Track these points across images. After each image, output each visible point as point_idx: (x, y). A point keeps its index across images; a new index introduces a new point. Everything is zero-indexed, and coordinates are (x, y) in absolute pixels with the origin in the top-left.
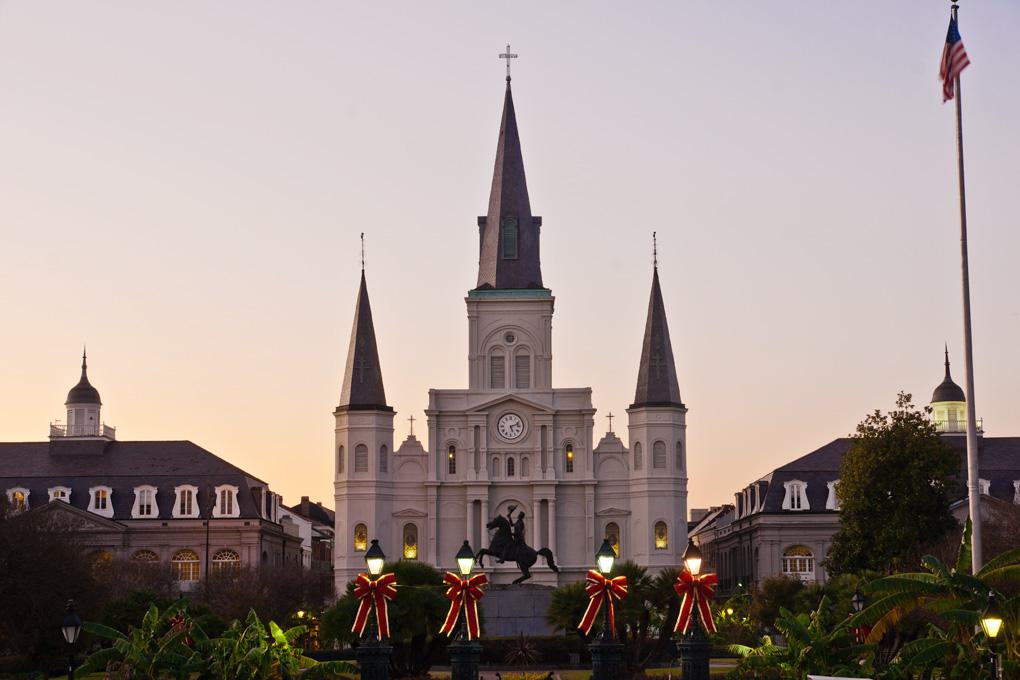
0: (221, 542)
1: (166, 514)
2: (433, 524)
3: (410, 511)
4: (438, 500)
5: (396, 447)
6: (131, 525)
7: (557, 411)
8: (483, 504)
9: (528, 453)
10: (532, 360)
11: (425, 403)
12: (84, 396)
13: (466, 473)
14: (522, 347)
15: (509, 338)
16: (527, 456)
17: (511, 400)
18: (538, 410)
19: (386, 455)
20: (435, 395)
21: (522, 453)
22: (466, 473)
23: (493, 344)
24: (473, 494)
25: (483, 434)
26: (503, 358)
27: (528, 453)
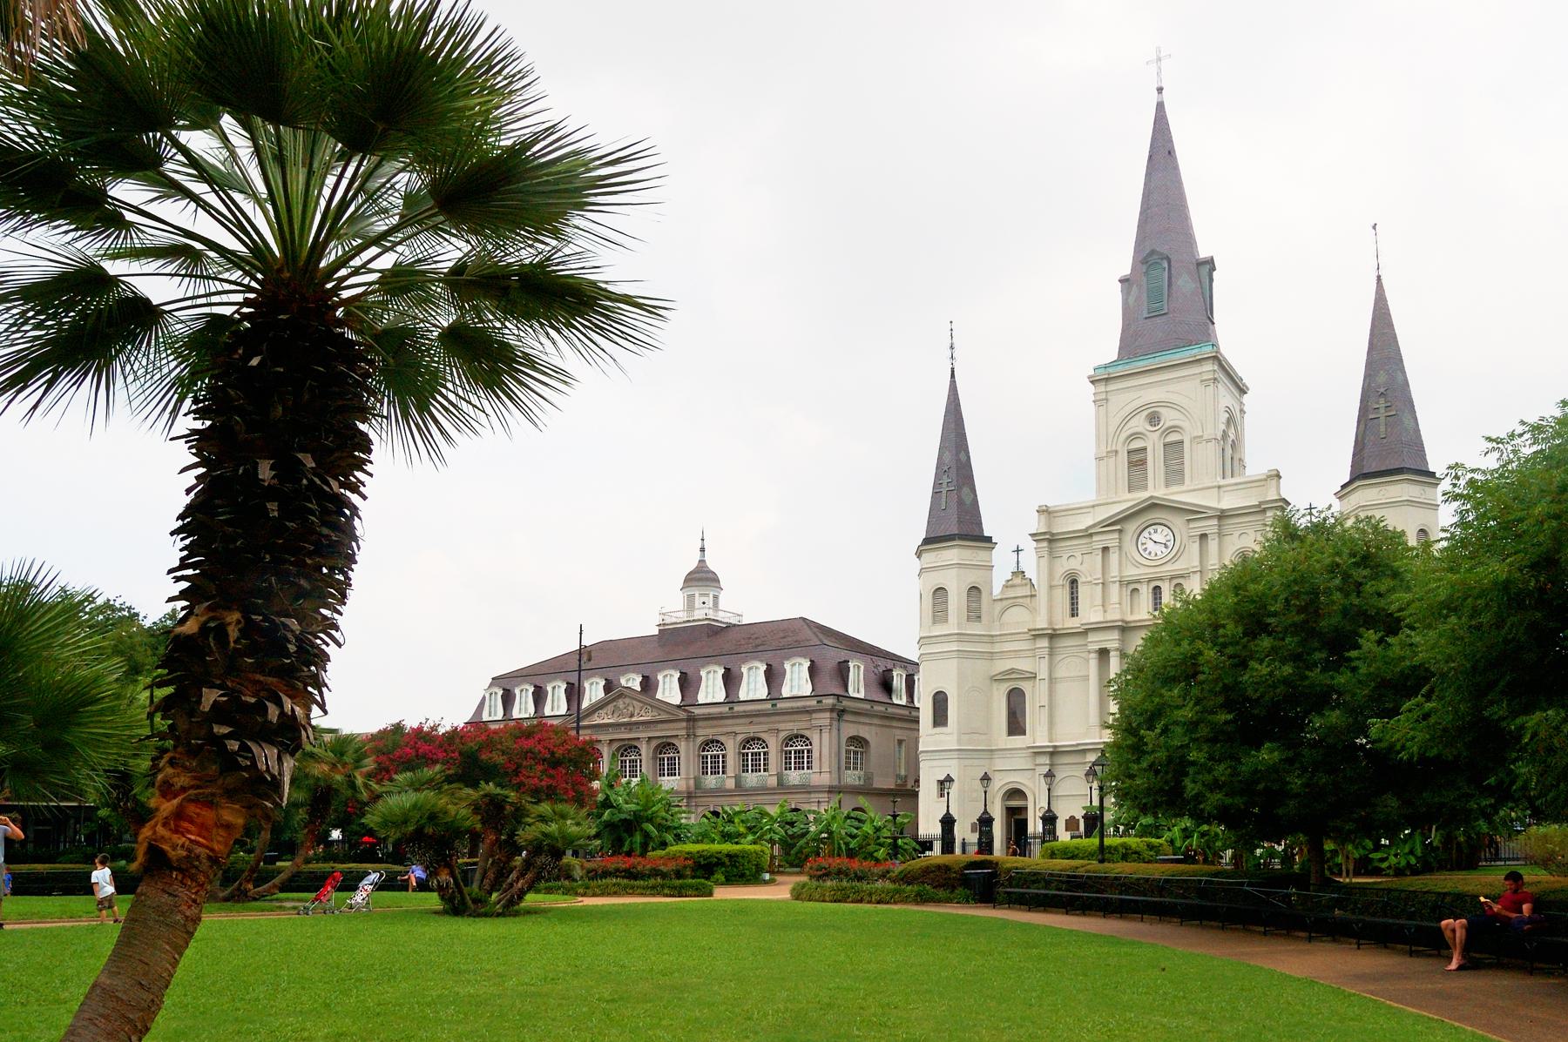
0: (790, 726)
1: (731, 699)
2: (1044, 686)
3: (1012, 671)
4: (1051, 655)
5: (997, 590)
6: (697, 711)
7: (1223, 511)
8: (1112, 654)
9: (1182, 576)
10: (1187, 445)
11: (1035, 524)
12: (702, 578)
13: (1090, 613)
14: (1174, 429)
15: (1154, 419)
16: (1180, 581)
17: (1153, 506)
18: (1191, 513)
19: (979, 600)
20: (1044, 511)
21: (1172, 578)
22: (1090, 613)
23: (1129, 432)
24: (1096, 641)
25: (1114, 557)
26: (1145, 449)
27: (1182, 576)
